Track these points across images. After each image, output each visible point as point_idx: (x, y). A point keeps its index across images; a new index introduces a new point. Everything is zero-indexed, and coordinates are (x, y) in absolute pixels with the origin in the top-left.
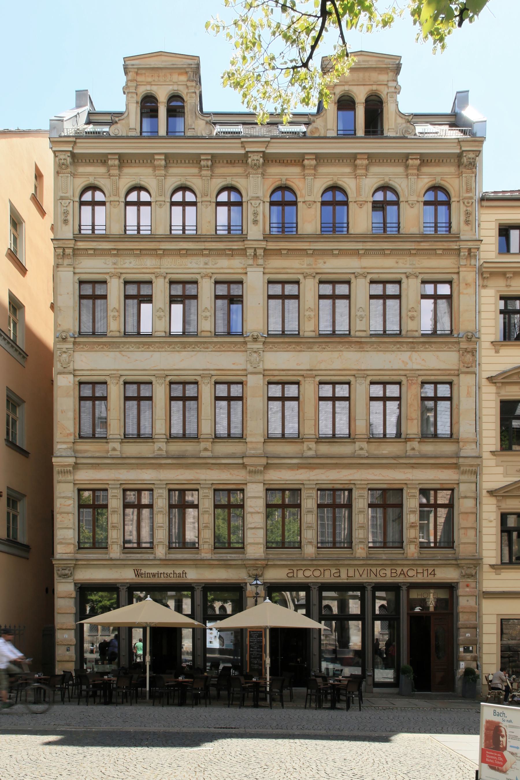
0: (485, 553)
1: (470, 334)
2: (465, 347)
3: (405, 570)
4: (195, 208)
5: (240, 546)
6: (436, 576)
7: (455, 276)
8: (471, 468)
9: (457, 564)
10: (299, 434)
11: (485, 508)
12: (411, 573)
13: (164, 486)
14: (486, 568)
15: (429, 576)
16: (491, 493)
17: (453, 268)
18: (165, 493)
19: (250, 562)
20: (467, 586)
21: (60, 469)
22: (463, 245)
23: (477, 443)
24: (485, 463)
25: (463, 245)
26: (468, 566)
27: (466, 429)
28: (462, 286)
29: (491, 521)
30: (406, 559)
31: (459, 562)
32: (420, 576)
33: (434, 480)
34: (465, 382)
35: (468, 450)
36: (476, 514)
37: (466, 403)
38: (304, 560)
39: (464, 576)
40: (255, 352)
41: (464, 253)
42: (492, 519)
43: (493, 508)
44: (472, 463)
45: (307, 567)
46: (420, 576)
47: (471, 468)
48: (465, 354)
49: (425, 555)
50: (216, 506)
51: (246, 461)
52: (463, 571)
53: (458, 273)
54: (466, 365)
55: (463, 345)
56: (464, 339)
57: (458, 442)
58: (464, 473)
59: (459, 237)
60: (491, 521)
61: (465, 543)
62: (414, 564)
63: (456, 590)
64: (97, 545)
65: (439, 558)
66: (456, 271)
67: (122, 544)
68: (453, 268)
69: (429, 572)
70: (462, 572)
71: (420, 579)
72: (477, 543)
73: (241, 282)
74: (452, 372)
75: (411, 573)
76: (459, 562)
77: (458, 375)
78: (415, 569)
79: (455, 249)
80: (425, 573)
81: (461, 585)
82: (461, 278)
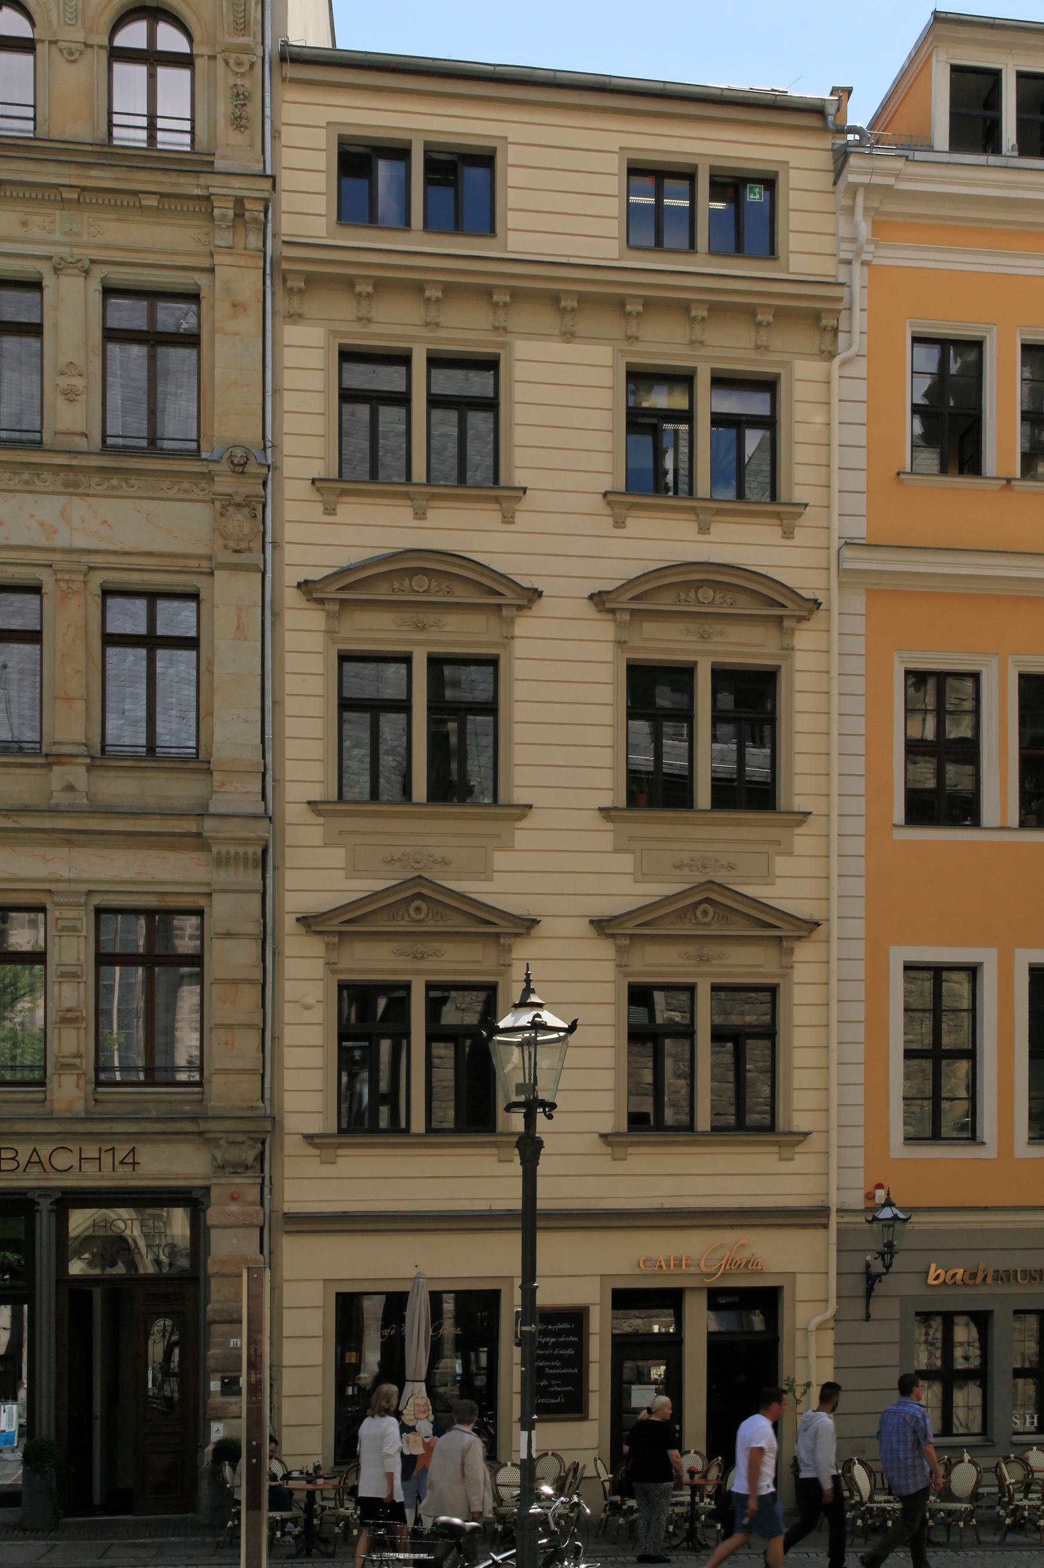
0: (290, 1102)
1: (239, 452)
2: (228, 491)
3: (45, 1150)
4: (186, 74)
5: (37, 1075)
6: (141, 1170)
7: (202, 280)
8: (241, 850)
9: (201, 1134)
10: (197, 748)
11: (291, 967)
12: (61, 1160)
13: (82, 900)
14: (292, 1145)
15: (121, 1170)
16: (308, 922)
17: (196, 254)
18: (86, 921)
19: (228, 1125)
20: (234, 1198)
21: (224, 851)
22: (216, 186)
23: (267, 776)
24: (291, 835)
25: (216, 186)
26: (232, 1137)
27: (233, 734)
28: (222, 309)
29: (308, 1007)
30: (49, 1118)
31: (203, 1126)
32: (90, 1168)
33: (134, 882)
34: (231, 595)
35: (237, 794)
36: (265, 984)
37: (232, 655)
38: (49, 1118)
39: (223, 1167)
40: (238, 506)
41: (224, 210)
42: (310, 1000)
43: (316, 968)
44: (244, 834)
45: (63, 1139)
46: (90, 1168)
47: (241, 850)
48: (231, 509)
49: (110, 1107)
50: (103, 959)
51: (210, 826)
52: (218, 1154)
53: (211, 270)
54: (233, 545)
55: (225, 484)
56: (225, 467)
57: (209, 772)
58: (222, 862)
59: (212, 162)
60: (308, 1007)
61: (226, 1071)
62: (71, 1131)
63: (205, 1211)
64: (159, 1076)
65: (154, 1114)
66: (205, 263)
67: (92, 1074)
68: (196, 254)
69: (120, 1155)
70: (214, 1159)
71: (89, 1177)
72: (266, 1071)
73: (193, 297)
74: (193, 563)
75: (61, 1160)
76: (203, 1126)
77: (212, 574)
78: (75, 1148)
79: (198, 197)
80: (107, 1159)
81: (214, 1194)
82: (218, 284)
